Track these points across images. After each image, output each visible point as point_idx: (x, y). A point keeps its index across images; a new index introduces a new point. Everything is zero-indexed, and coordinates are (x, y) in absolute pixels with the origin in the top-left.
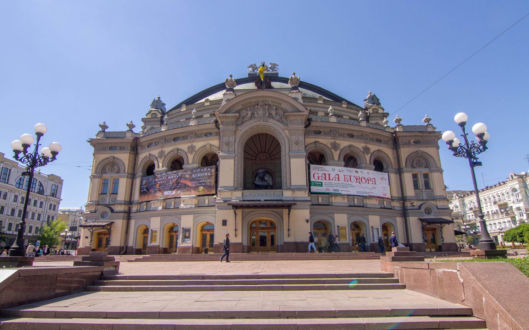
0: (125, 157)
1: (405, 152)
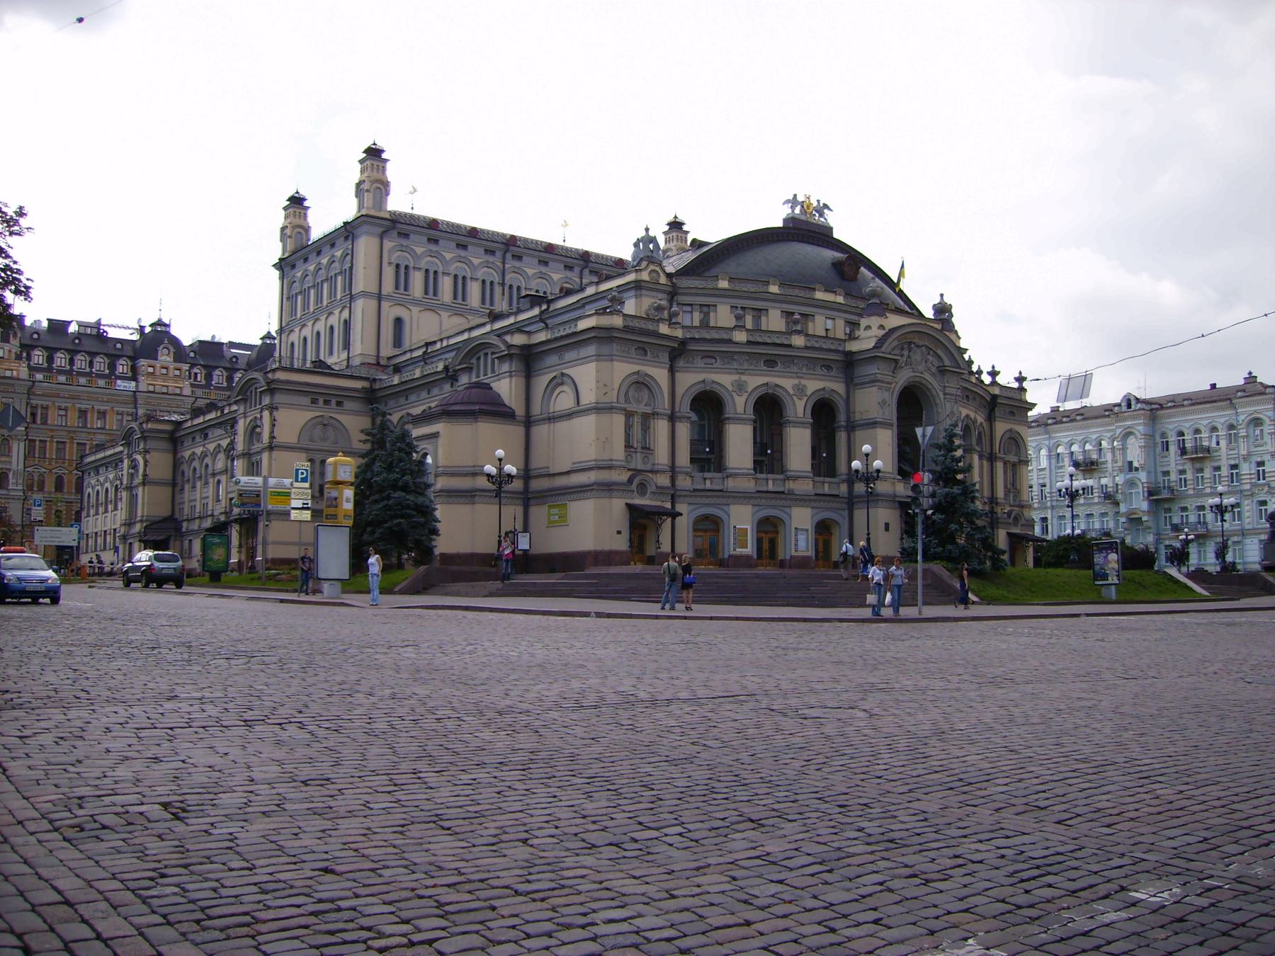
0: (660, 375)
1: (1001, 427)
